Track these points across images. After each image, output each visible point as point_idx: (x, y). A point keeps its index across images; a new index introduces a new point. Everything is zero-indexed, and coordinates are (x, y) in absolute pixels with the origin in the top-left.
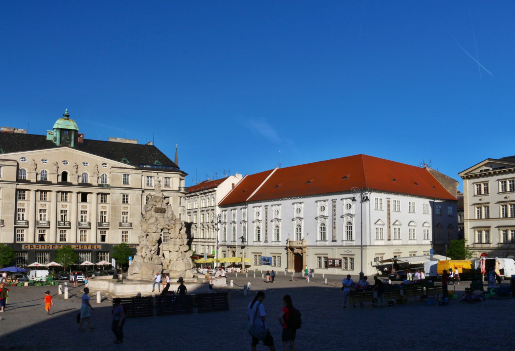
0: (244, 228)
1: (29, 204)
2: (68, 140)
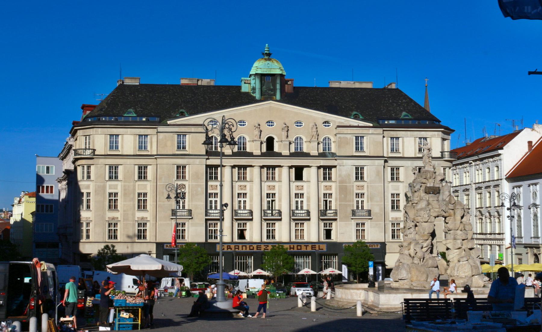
2: (272, 90)
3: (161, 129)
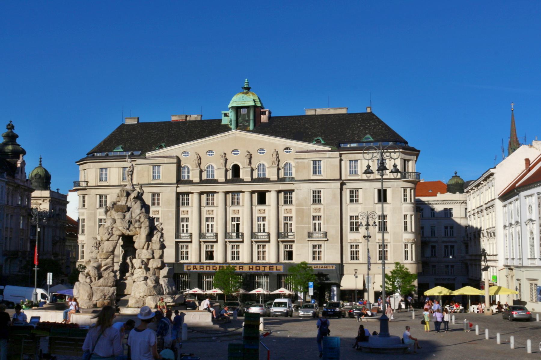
1: (191, 212)
3: (139, 161)
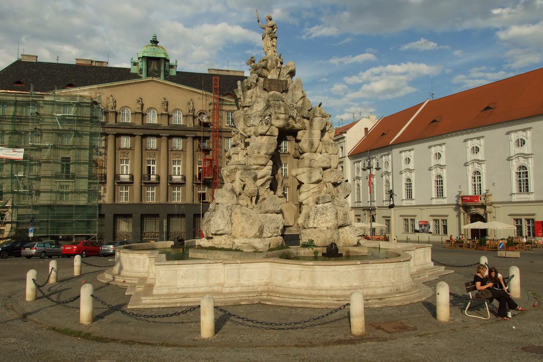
0: (387, 182)
2: (157, 72)
